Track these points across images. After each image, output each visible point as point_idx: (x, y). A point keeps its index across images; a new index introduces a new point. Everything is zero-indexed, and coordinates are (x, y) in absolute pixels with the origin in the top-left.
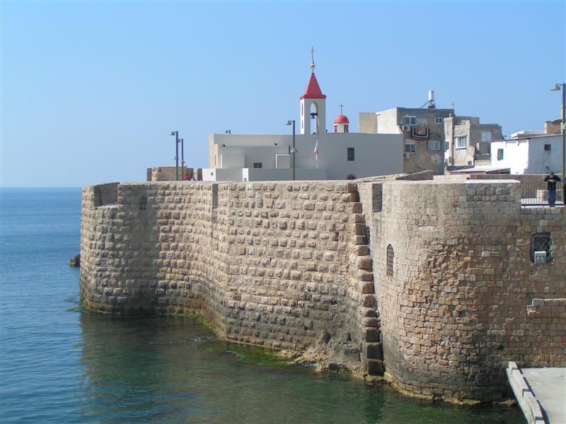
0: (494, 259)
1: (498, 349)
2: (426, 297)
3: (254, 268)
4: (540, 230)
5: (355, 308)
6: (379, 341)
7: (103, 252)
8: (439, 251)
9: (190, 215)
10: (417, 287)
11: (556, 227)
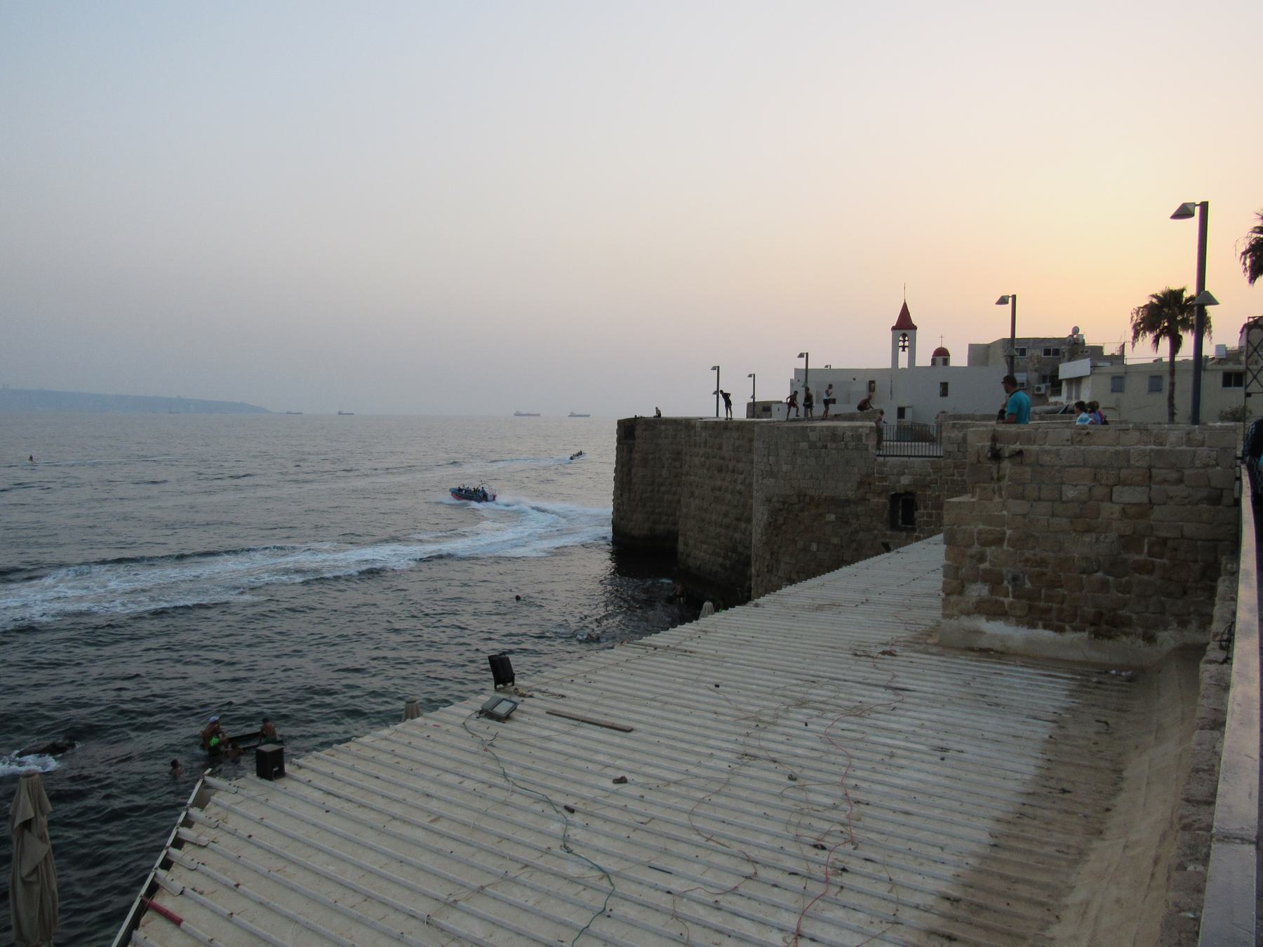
2: (767, 566)
8: (781, 510)
10: (760, 553)
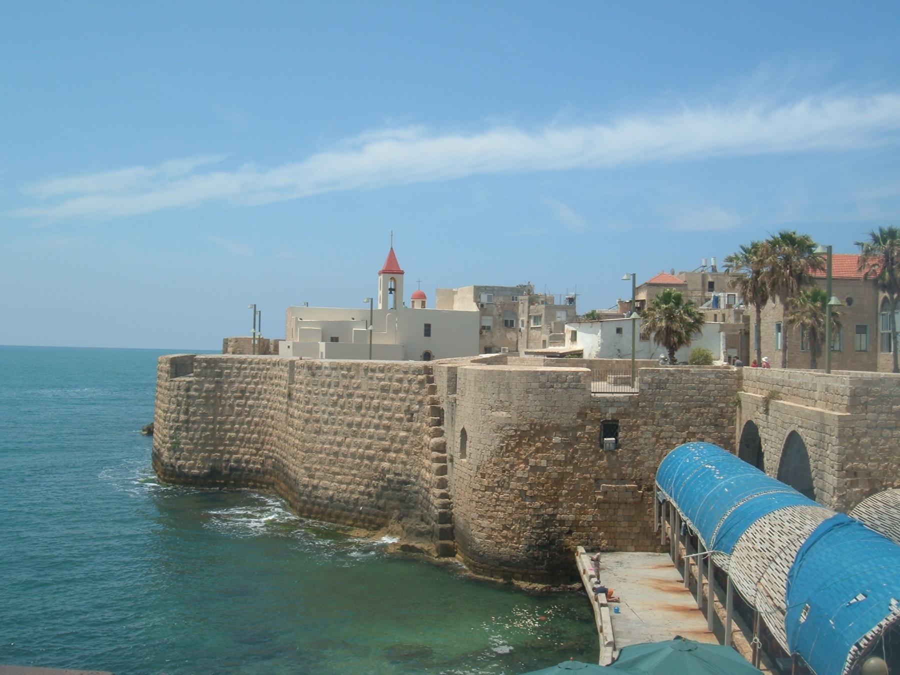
0: (567, 445)
1: (567, 533)
3: (328, 446)
4: (609, 417)
5: (427, 490)
6: (451, 523)
7: (177, 424)
8: (512, 436)
9: (266, 390)
11: (626, 414)
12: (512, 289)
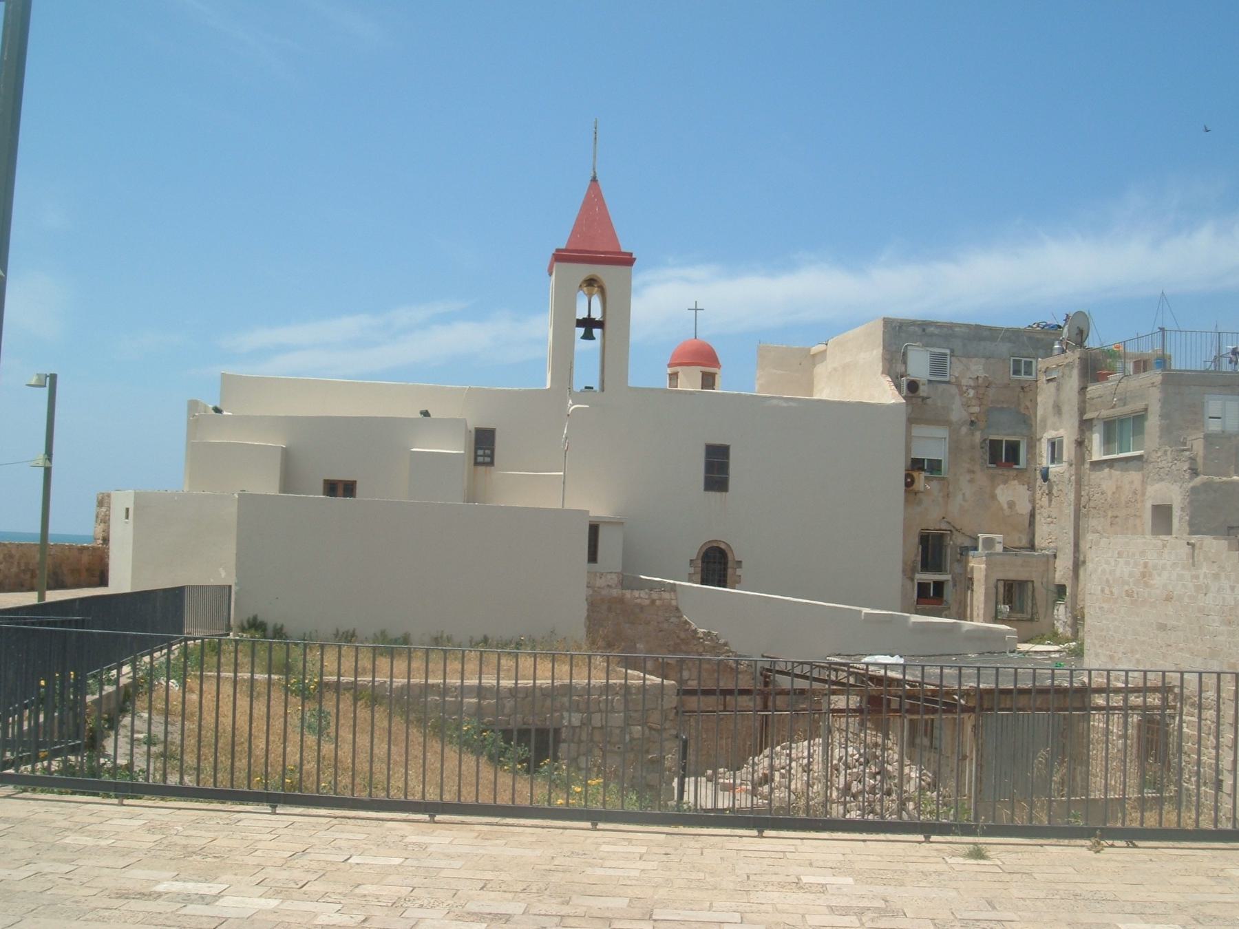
12: (1013, 335)
